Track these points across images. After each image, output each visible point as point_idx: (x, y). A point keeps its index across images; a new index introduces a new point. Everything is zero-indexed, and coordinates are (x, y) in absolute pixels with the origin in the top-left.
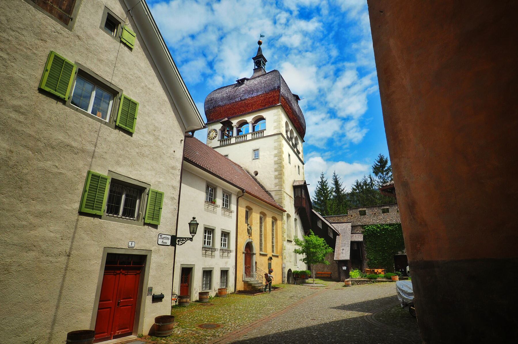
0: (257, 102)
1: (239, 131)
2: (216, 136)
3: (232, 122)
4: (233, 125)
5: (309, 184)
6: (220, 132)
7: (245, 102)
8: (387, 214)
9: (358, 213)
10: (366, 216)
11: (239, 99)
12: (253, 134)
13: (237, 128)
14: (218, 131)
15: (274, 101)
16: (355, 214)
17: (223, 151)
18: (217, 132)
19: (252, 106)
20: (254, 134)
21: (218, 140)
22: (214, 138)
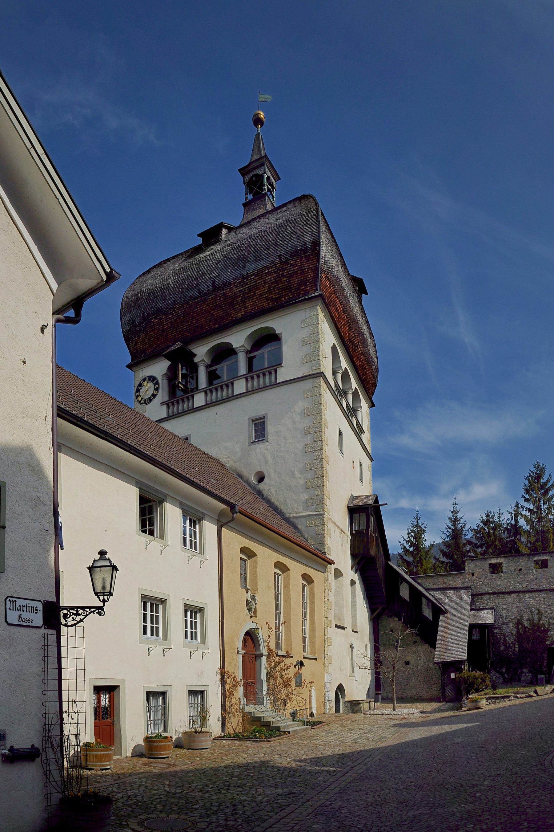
0: (258, 289)
1: (213, 376)
2: (155, 392)
3: (195, 351)
6: (166, 382)
7: (225, 294)
11: (208, 287)
12: (250, 379)
13: (207, 367)
15: (302, 285)
18: (157, 383)
20: (252, 378)
21: (162, 404)
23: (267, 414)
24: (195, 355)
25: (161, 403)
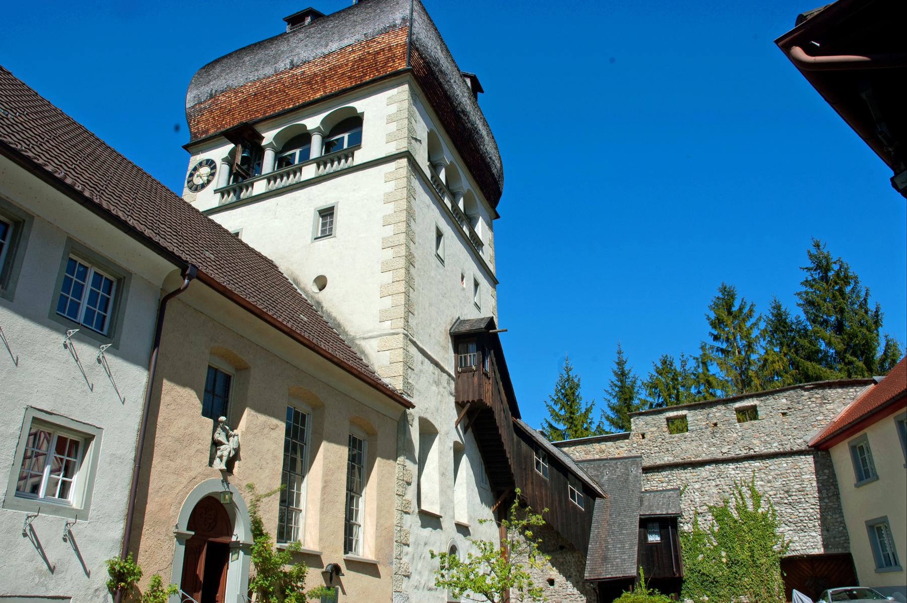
4: (264, 143)
8: (753, 425)
10: (687, 433)
14: (218, 162)
17: (228, 221)
19: (324, 82)
21: (216, 191)
23: (338, 202)
24: (263, 138)
25: (215, 191)
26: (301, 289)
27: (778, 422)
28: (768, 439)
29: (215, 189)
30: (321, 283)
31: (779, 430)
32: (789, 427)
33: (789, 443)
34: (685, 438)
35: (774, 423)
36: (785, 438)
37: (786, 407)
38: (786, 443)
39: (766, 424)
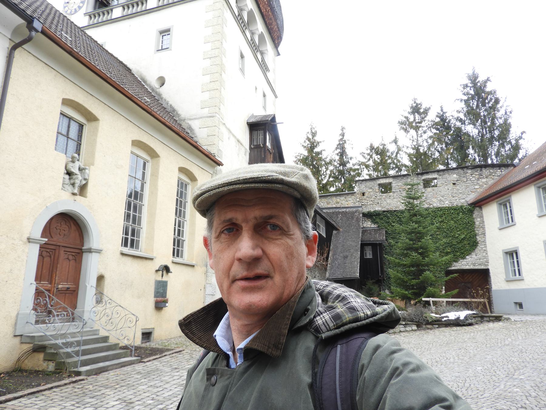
2: (81, 5)
5: (283, 123)
8: (433, 190)
9: (377, 187)
10: (391, 194)
16: (371, 190)
22: (77, 9)
25: (84, 14)
26: (147, 85)
27: (450, 189)
28: (442, 199)
29: (85, 13)
30: (162, 81)
31: (450, 194)
32: (457, 192)
33: (456, 202)
34: (390, 196)
35: (447, 189)
36: (453, 198)
37: (456, 180)
38: (454, 201)
39: (442, 189)
